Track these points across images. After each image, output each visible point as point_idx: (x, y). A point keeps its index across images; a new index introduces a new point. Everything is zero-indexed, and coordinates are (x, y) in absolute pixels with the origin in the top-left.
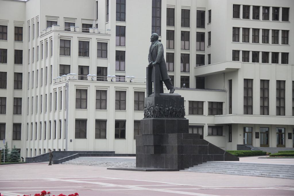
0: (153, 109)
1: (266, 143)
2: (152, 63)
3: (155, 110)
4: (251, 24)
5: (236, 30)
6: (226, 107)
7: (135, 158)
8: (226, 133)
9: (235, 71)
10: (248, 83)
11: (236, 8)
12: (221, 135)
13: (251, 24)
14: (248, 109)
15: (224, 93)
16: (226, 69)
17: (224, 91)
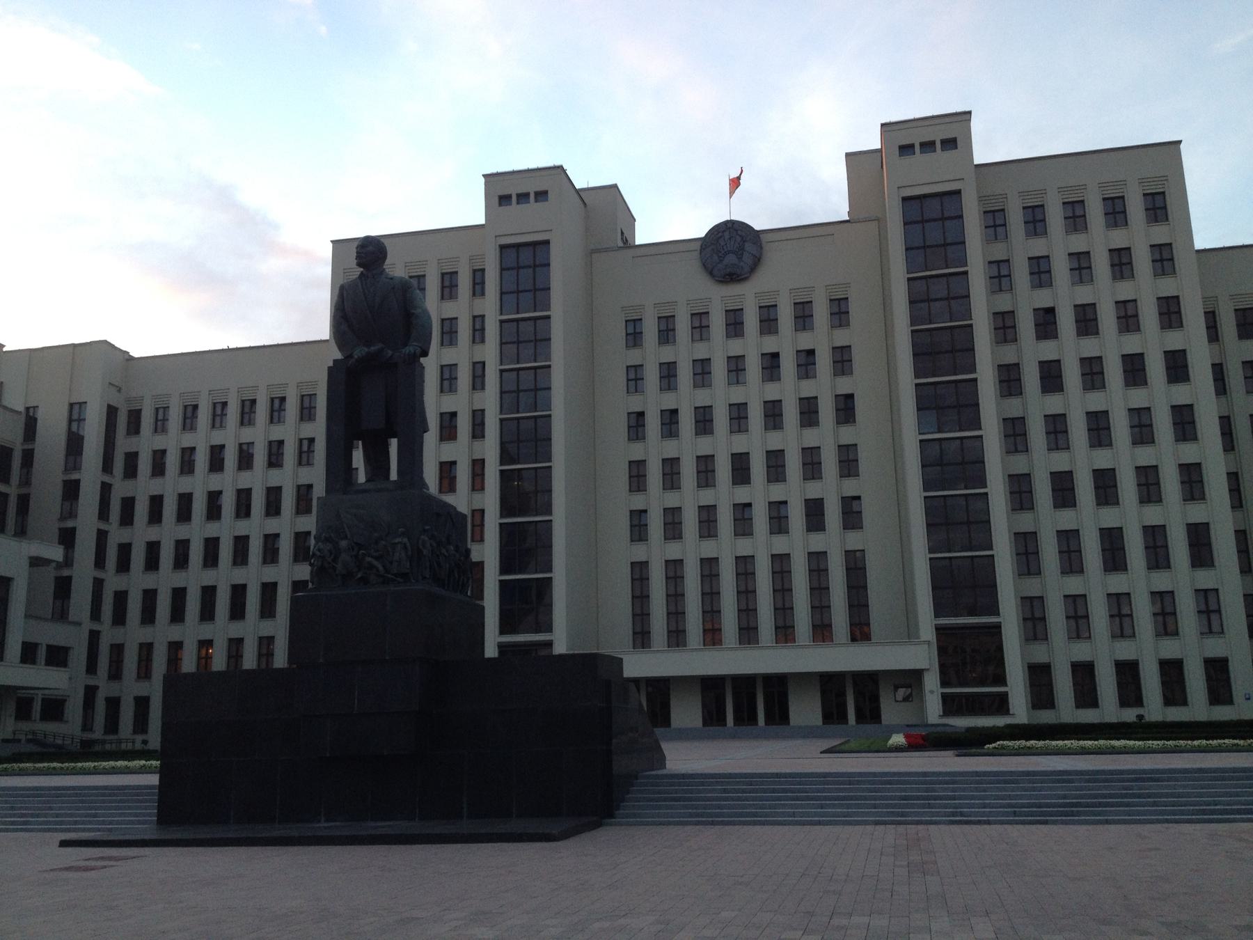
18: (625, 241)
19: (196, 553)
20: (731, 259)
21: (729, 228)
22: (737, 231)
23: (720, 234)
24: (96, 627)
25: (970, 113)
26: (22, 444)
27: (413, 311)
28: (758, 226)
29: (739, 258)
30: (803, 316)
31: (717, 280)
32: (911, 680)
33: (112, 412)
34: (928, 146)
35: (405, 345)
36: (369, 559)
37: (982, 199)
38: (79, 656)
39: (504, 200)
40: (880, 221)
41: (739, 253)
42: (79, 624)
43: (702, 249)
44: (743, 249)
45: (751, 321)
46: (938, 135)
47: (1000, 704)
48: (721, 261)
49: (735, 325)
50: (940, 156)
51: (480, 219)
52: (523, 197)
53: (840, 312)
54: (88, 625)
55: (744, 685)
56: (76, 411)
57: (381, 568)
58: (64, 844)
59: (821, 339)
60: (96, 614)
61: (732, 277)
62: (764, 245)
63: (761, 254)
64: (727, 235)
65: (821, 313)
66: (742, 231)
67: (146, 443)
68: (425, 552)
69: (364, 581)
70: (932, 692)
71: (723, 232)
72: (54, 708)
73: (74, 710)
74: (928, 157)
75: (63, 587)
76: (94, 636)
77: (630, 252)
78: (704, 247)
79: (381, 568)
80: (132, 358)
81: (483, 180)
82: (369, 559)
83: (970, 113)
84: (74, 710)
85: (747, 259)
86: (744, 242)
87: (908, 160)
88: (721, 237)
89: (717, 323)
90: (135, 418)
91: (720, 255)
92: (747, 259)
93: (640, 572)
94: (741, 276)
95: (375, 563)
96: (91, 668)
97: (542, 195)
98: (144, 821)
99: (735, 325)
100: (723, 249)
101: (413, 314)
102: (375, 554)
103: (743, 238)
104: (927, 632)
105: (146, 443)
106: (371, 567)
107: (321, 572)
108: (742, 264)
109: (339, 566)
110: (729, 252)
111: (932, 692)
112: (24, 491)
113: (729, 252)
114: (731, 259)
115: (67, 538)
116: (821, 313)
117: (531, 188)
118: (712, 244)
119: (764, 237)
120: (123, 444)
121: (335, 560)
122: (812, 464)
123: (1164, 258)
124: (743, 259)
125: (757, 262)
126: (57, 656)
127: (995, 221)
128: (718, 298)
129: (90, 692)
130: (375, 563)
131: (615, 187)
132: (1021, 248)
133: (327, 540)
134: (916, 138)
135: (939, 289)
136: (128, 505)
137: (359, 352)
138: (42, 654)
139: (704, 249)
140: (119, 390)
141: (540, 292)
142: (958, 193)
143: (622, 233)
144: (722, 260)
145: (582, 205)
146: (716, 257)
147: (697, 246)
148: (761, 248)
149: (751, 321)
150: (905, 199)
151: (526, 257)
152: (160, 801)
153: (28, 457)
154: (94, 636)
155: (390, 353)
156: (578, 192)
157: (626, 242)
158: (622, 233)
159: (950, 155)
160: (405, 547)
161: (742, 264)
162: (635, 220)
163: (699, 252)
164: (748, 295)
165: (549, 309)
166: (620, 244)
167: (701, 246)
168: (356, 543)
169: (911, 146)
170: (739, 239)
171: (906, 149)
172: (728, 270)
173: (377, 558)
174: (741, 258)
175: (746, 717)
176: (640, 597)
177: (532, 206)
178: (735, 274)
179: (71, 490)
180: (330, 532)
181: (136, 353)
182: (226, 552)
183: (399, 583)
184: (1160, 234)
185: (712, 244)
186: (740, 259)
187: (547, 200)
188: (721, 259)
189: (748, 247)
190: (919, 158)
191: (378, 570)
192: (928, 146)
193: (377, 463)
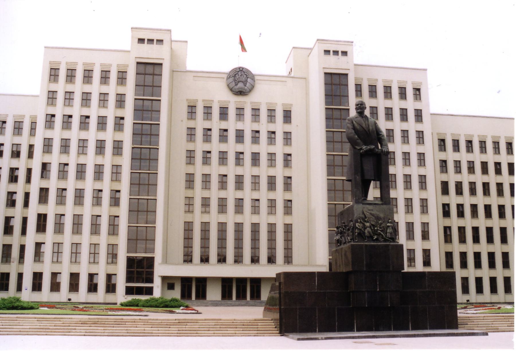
20: (240, 85)
21: (241, 70)
22: (244, 72)
23: (237, 73)
27: (380, 133)
29: (245, 85)
31: (233, 93)
37: (356, 79)
39: (141, 41)
41: (245, 83)
43: (228, 78)
44: (247, 81)
45: (248, 113)
46: (340, 49)
48: (236, 85)
53: (287, 116)
55: (241, 282)
59: (279, 127)
61: (241, 93)
62: (256, 81)
63: (254, 84)
66: (246, 72)
69: (377, 240)
71: (238, 72)
74: (336, 57)
78: (229, 77)
86: (248, 78)
87: (327, 57)
88: (237, 74)
91: (236, 82)
93: (188, 227)
94: (244, 93)
97: (160, 41)
100: (238, 80)
101: (381, 134)
102: (381, 229)
103: (247, 76)
108: (246, 88)
110: (241, 81)
113: (241, 81)
114: (240, 85)
118: (233, 76)
119: (256, 78)
123: (419, 115)
124: (247, 86)
125: (253, 87)
130: (382, 233)
135: (337, 114)
139: (229, 78)
141: (156, 87)
142: (346, 75)
144: (237, 85)
146: (234, 83)
147: (225, 76)
148: (254, 81)
149: (248, 113)
150: (326, 73)
151: (150, 69)
156: (171, 41)
159: (344, 58)
163: (225, 79)
165: (160, 96)
167: (228, 76)
168: (372, 224)
170: (245, 76)
171: (327, 52)
172: (241, 90)
174: (246, 85)
175: (241, 296)
176: (188, 238)
177: (155, 46)
178: (243, 92)
183: (391, 241)
186: (245, 85)
187: (163, 44)
188: (236, 84)
189: (249, 80)
191: (382, 236)
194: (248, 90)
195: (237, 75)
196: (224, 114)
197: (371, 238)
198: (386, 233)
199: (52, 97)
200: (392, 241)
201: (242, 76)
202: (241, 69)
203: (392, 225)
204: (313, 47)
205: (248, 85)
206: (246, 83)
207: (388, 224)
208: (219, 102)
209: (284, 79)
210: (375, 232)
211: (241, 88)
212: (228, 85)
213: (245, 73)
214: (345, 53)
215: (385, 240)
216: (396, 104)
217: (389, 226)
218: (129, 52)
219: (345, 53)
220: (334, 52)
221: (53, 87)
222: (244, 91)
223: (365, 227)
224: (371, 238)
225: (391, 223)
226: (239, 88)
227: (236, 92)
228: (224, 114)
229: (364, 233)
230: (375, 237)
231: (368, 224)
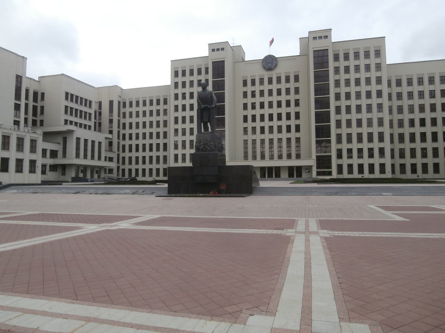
0: (214, 144)
1: (85, 175)
2: (207, 106)
3: (216, 145)
4: (73, 105)
5: (66, 107)
6: (60, 154)
7: (166, 185)
8: (60, 170)
9: (70, 132)
10: (78, 139)
11: (67, 94)
12: (56, 171)
13: (73, 105)
14: (78, 156)
15: (59, 145)
16: (67, 130)
17: (60, 143)
18: (243, 59)
19: (141, 136)
22: (271, 57)
24: (119, 153)
25: (331, 29)
26: (98, 110)
28: (277, 56)
30: (288, 80)
32: (309, 168)
33: (119, 102)
34: (320, 37)
35: (212, 105)
36: (206, 147)
37: (333, 51)
38: (115, 160)
39: (213, 50)
40: (307, 55)
41: (272, 63)
42: (115, 152)
43: (262, 62)
44: (273, 62)
45: (274, 80)
46: (323, 35)
47: (330, 173)
48: (267, 65)
49: (270, 81)
50: (323, 40)
51: (207, 54)
52: (218, 50)
53: (297, 79)
54: (117, 152)
56: (111, 103)
57: (209, 148)
58: (156, 196)
59: (292, 85)
60: (118, 150)
61: (270, 69)
62: (278, 61)
63: (277, 63)
64: (269, 58)
65: (292, 79)
67: (128, 110)
68: (217, 146)
69: (206, 151)
70: (314, 171)
71: (268, 58)
72: (111, 171)
73: (115, 171)
75: (111, 144)
76: (118, 155)
77: (244, 63)
79: (209, 148)
80: (123, 89)
81: (208, 45)
82: (206, 147)
83: (331, 29)
84: (115, 171)
85: (274, 65)
87: (315, 41)
89: (266, 81)
90: (124, 104)
92: (274, 65)
95: (208, 147)
96: (118, 162)
97: (223, 49)
98: (166, 193)
99: (270, 81)
104: (314, 157)
105: (128, 110)
106: (207, 148)
107: (197, 149)
108: (272, 66)
109: (201, 148)
110: (269, 63)
111: (314, 171)
112: (100, 121)
113: (269, 63)
114: (270, 65)
115: (111, 132)
116: (292, 79)
117: (220, 47)
119: (278, 59)
120: (122, 110)
121: (200, 147)
122: (288, 116)
124: (273, 65)
125: (276, 65)
126: (111, 159)
127: (336, 58)
128: (266, 75)
129: (118, 168)
130: (208, 147)
131: (241, 46)
132: (342, 64)
133: (198, 143)
134: (317, 35)
136: (124, 124)
137: (203, 106)
138: (108, 159)
140: (120, 97)
142: (327, 49)
143: (242, 57)
145: (232, 50)
147: (261, 61)
148: (277, 62)
149: (274, 80)
150: (314, 51)
152: (168, 190)
153: (100, 114)
154: (118, 155)
155: (209, 106)
156: (231, 47)
157: (243, 60)
158: (242, 57)
160: (213, 145)
161: (272, 66)
162: (245, 53)
163: (262, 63)
164: (274, 74)
166: (242, 61)
169: (316, 37)
170: (272, 60)
171: (315, 38)
172: (269, 67)
173: (207, 146)
175: (270, 176)
176: (246, 148)
177: (220, 51)
179: (111, 121)
180: (199, 140)
181: (123, 88)
182: (148, 136)
184: (378, 61)
185: (265, 61)
186: (272, 65)
189: (274, 62)
190: (318, 40)
191: (208, 149)
192: (320, 37)
193: (206, 128)
194: (274, 67)
195: (267, 60)
196: (262, 81)
197: (202, 150)
198: (211, 147)
199: (176, 85)
200: (212, 151)
201: (270, 60)
202: (270, 56)
203: (213, 143)
204: (308, 36)
205: (274, 64)
206: (272, 63)
207: (212, 143)
208: (259, 75)
209: (294, 58)
210: (205, 147)
211: (270, 66)
212: (263, 66)
213: (272, 58)
214: (326, 37)
215: (210, 151)
216: (362, 62)
217: (211, 144)
218: (208, 56)
219: (326, 37)
220: (319, 37)
221: (176, 80)
222: (272, 68)
223: (200, 145)
224: (202, 150)
225: (213, 142)
226: (269, 66)
227: (267, 69)
228: (262, 81)
229: (200, 148)
230: (205, 150)
231: (202, 144)
